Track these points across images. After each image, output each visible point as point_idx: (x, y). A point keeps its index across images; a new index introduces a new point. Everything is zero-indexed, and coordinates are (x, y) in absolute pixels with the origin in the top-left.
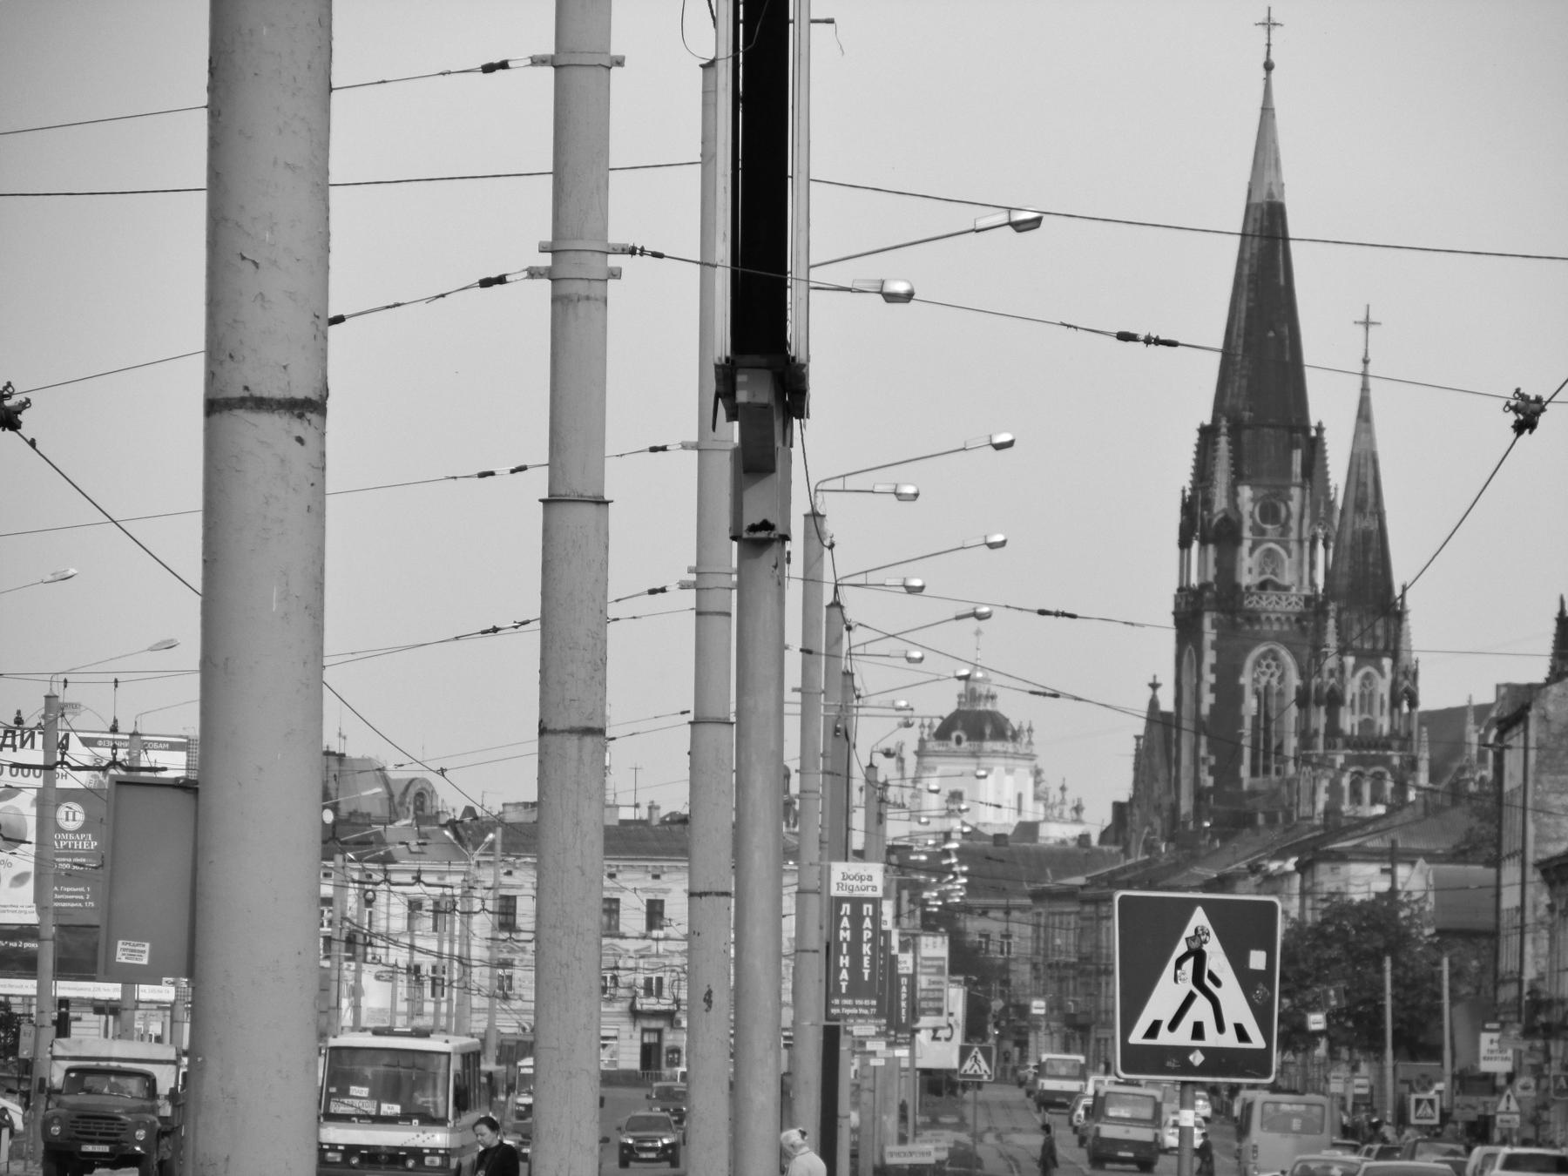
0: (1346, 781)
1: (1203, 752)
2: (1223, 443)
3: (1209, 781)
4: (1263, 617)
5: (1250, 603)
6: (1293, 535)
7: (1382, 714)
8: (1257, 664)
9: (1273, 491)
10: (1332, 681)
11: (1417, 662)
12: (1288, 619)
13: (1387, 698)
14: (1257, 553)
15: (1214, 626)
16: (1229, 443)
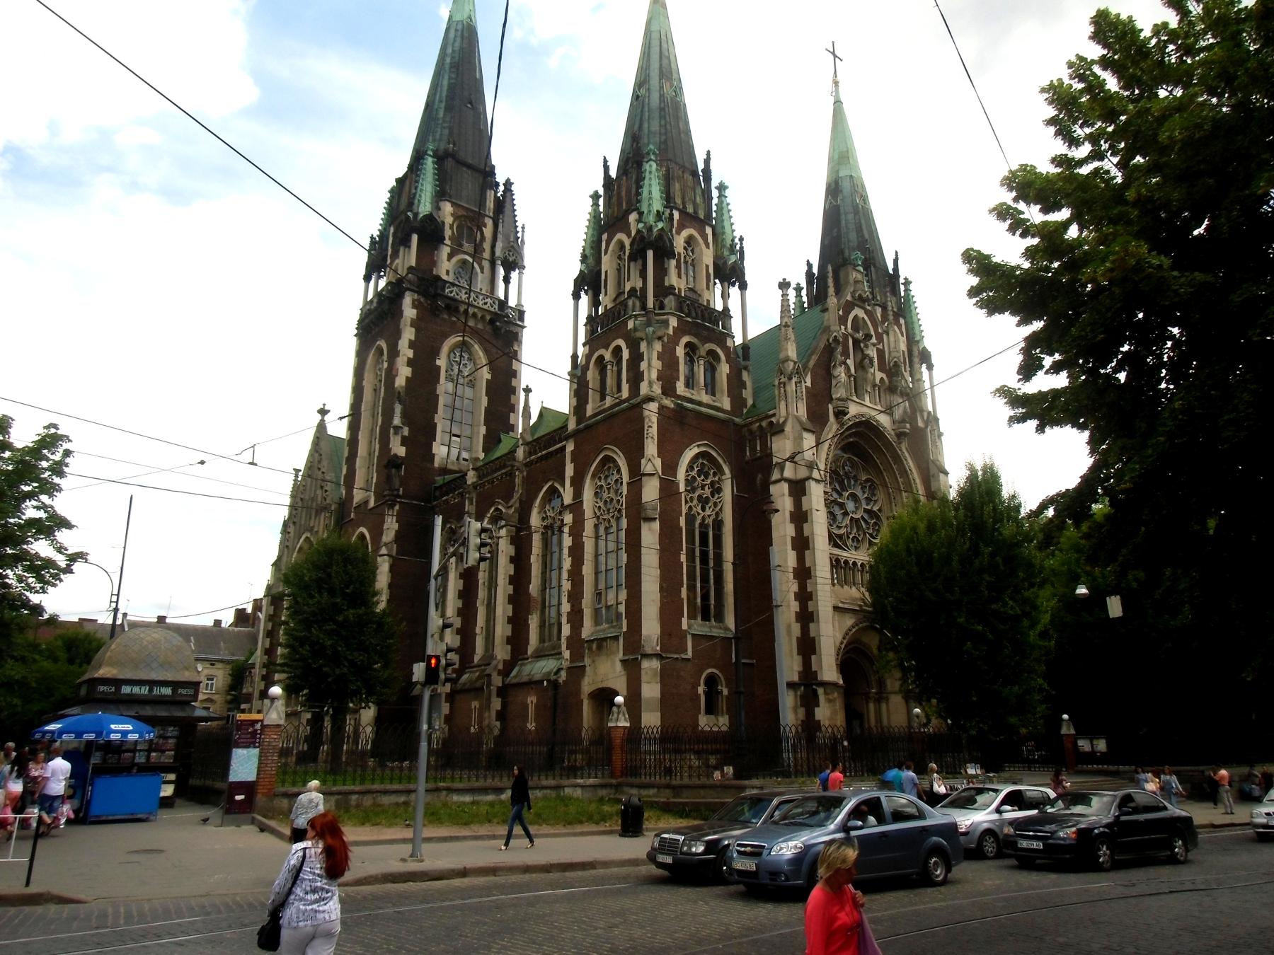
0: (680, 351)
1: (397, 421)
2: (429, 163)
3: (401, 451)
4: (462, 308)
5: (451, 292)
6: (487, 255)
8: (452, 350)
9: (471, 214)
10: (660, 225)
11: (741, 239)
12: (483, 317)
13: (711, 270)
14: (454, 260)
15: (415, 305)
16: (433, 162)
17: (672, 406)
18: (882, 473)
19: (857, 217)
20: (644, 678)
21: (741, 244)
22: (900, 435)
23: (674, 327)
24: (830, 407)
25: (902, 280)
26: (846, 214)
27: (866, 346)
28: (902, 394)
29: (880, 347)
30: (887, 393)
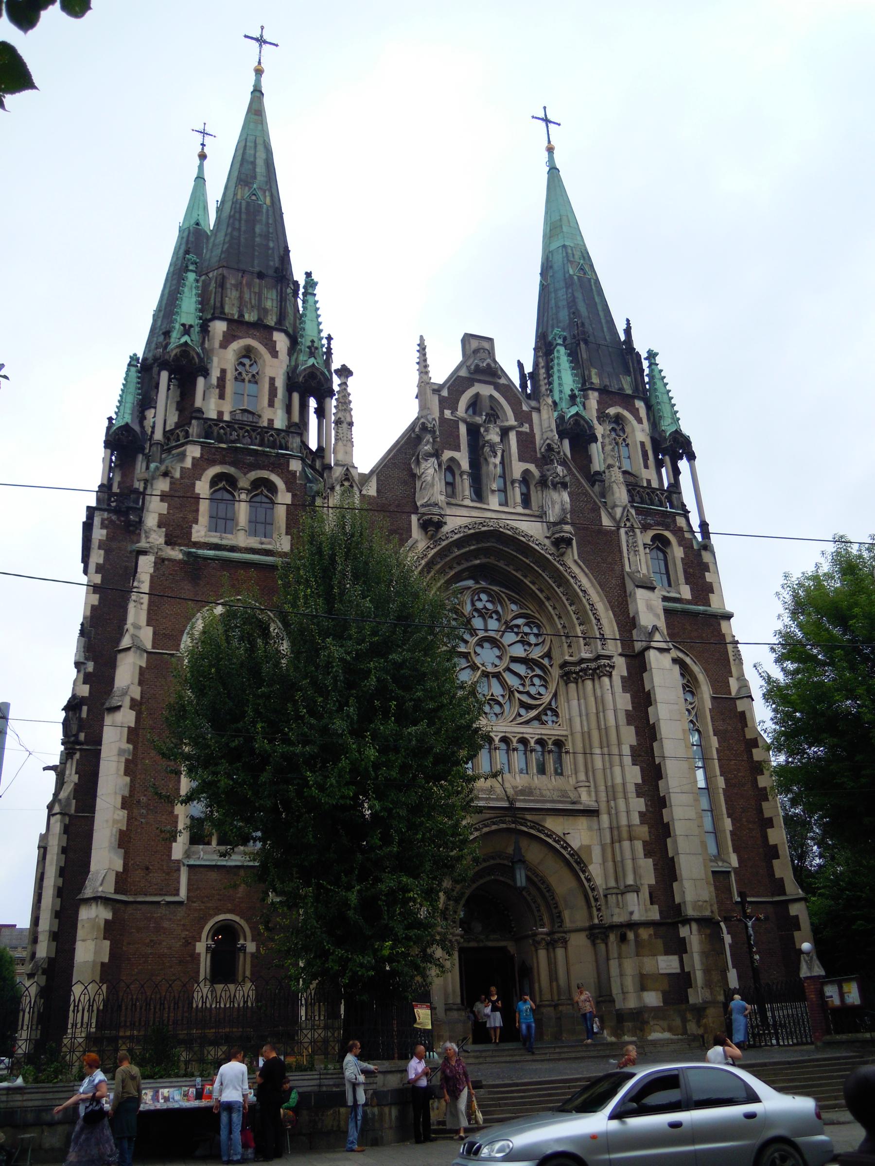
0: (202, 487)
7: (271, 404)
11: (329, 338)
13: (280, 383)
17: (180, 556)
18: (543, 603)
19: (570, 291)
20: (81, 933)
21: (329, 344)
22: (562, 543)
23: (194, 458)
24: (414, 518)
25: (644, 355)
26: (556, 291)
27: (487, 430)
28: (555, 486)
29: (526, 428)
30: (539, 488)
